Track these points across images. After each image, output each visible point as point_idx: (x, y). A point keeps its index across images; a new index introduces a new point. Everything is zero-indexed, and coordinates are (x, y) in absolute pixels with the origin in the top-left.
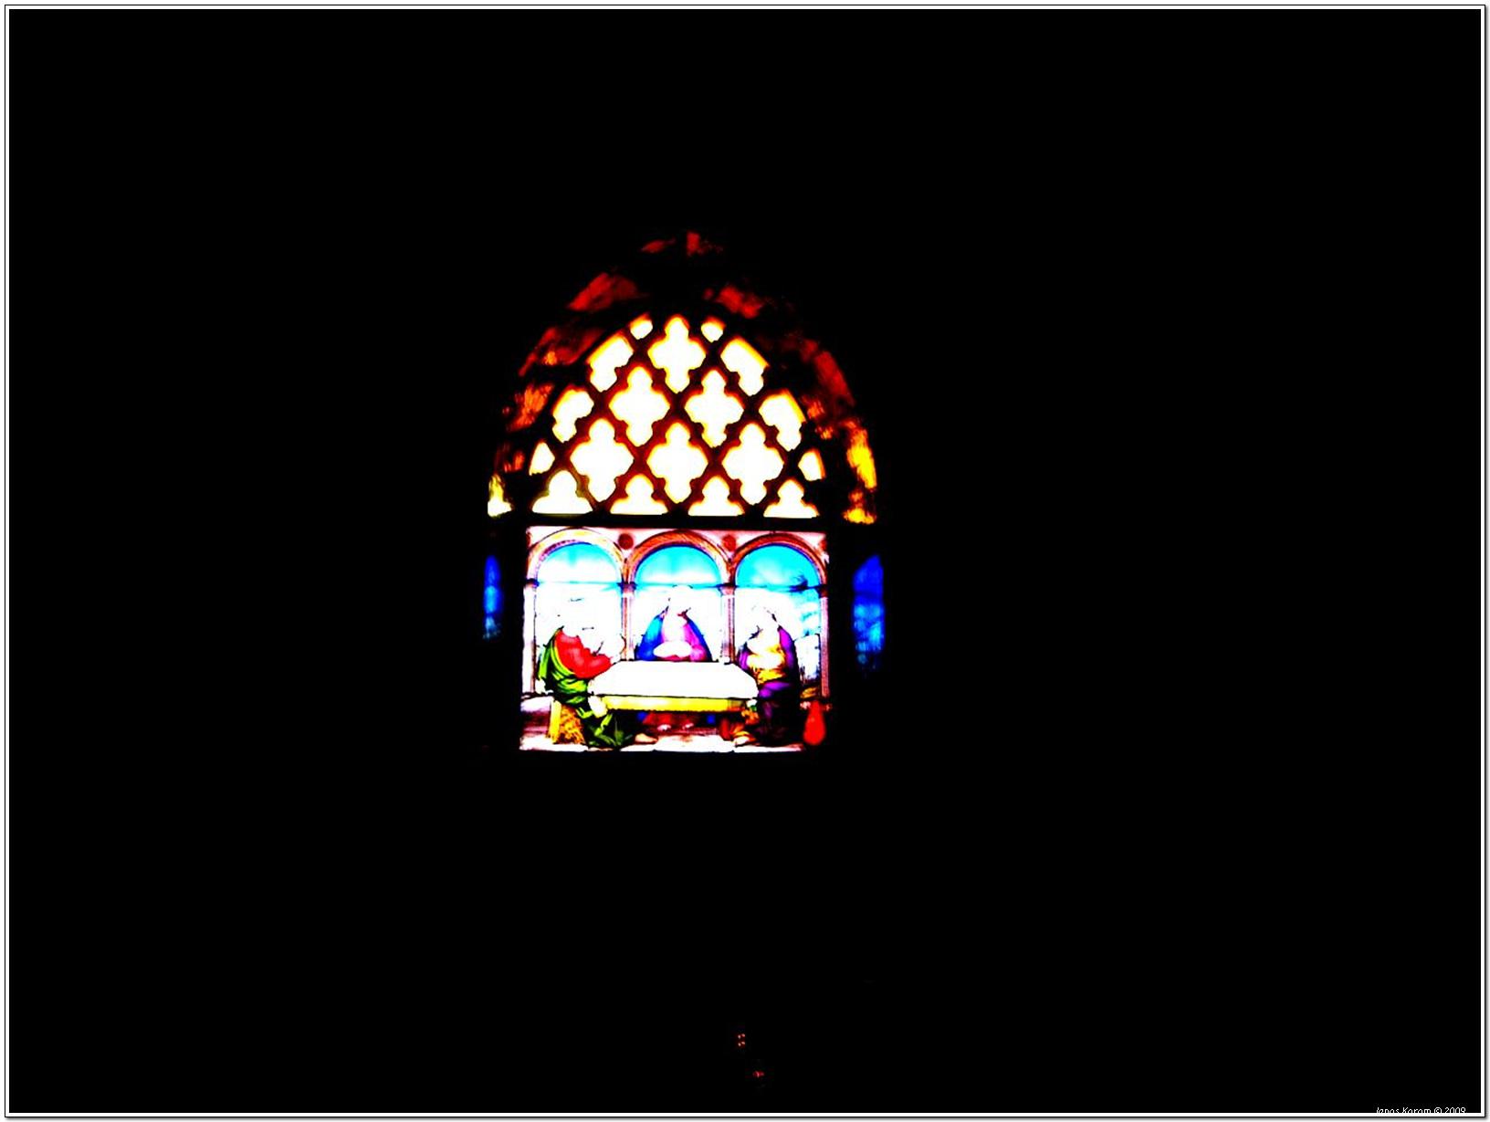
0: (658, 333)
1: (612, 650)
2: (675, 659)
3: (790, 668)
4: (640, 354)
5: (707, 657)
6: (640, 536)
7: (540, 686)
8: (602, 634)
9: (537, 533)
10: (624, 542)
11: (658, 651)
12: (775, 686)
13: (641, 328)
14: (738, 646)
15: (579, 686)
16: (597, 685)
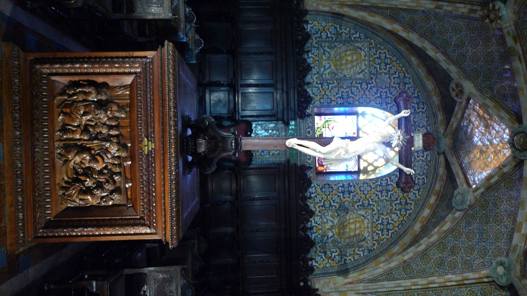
7: (327, 119)
15: (327, 126)
16: (327, 129)
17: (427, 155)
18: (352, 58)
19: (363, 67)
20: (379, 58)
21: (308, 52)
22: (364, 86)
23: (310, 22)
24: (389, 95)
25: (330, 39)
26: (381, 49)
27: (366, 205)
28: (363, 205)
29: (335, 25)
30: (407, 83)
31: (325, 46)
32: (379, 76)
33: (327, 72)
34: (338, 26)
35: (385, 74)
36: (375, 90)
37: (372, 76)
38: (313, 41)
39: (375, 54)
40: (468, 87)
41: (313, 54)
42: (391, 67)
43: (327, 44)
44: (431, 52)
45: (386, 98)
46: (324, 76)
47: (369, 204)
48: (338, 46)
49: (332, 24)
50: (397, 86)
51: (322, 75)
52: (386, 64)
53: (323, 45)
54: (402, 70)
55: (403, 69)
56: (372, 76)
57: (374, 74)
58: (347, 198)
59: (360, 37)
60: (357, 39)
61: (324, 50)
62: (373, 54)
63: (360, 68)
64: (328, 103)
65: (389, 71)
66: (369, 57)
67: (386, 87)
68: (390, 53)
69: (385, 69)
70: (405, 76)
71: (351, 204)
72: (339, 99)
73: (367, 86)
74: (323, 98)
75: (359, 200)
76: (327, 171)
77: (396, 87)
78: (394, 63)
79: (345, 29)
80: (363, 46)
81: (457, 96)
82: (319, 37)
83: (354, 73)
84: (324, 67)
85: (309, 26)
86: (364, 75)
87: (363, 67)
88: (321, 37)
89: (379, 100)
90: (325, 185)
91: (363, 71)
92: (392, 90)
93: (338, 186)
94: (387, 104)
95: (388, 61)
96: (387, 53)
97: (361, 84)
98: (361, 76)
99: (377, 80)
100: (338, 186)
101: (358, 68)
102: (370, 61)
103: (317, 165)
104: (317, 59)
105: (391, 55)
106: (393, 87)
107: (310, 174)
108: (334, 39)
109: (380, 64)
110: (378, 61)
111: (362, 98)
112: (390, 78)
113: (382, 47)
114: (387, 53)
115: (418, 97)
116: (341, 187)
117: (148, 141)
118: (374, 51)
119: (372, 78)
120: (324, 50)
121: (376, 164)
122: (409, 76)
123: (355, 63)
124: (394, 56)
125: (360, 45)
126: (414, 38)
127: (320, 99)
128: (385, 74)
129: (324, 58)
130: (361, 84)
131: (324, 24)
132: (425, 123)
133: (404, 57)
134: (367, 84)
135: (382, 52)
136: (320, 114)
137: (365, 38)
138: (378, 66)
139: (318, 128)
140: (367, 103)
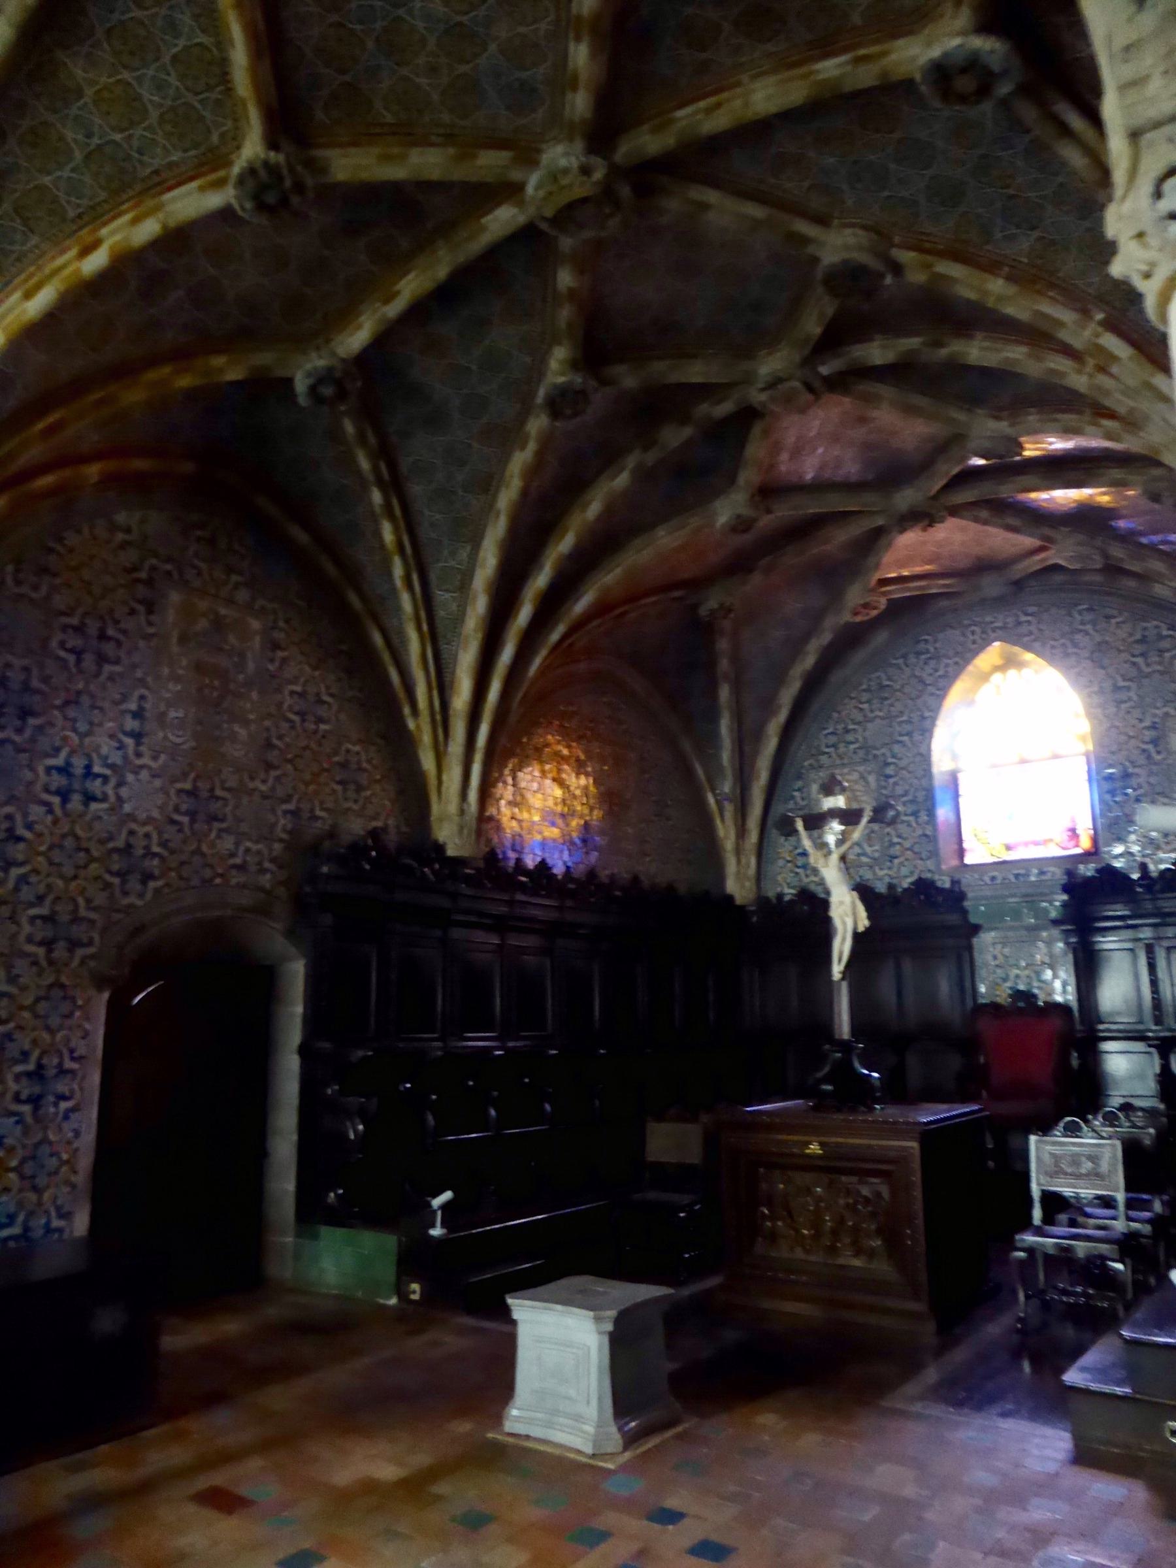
17: (1027, 614)
19: (855, 776)
22: (890, 770)
27: (1153, 733)
28: (1155, 742)
33: (868, 850)
40: (854, 595)
44: (809, 661)
46: (876, 855)
47: (1154, 727)
51: (875, 859)
57: (867, 753)
58: (1141, 780)
59: (799, 790)
71: (1154, 768)
72: (920, 820)
75: (1144, 751)
81: (875, 608)
84: (859, 855)
86: (869, 773)
87: (855, 776)
89: (917, 737)
91: (862, 777)
94: (923, 718)
97: (888, 777)
98: (872, 779)
103: (1078, 851)
107: (1087, 870)
110: (842, 749)
112: (871, 720)
115: (904, 656)
118: (824, 759)
119: (875, 756)
124: (830, 717)
126: (787, 697)
130: (888, 777)
131: (781, 863)
132: (957, 632)
134: (887, 764)
136: (961, 852)
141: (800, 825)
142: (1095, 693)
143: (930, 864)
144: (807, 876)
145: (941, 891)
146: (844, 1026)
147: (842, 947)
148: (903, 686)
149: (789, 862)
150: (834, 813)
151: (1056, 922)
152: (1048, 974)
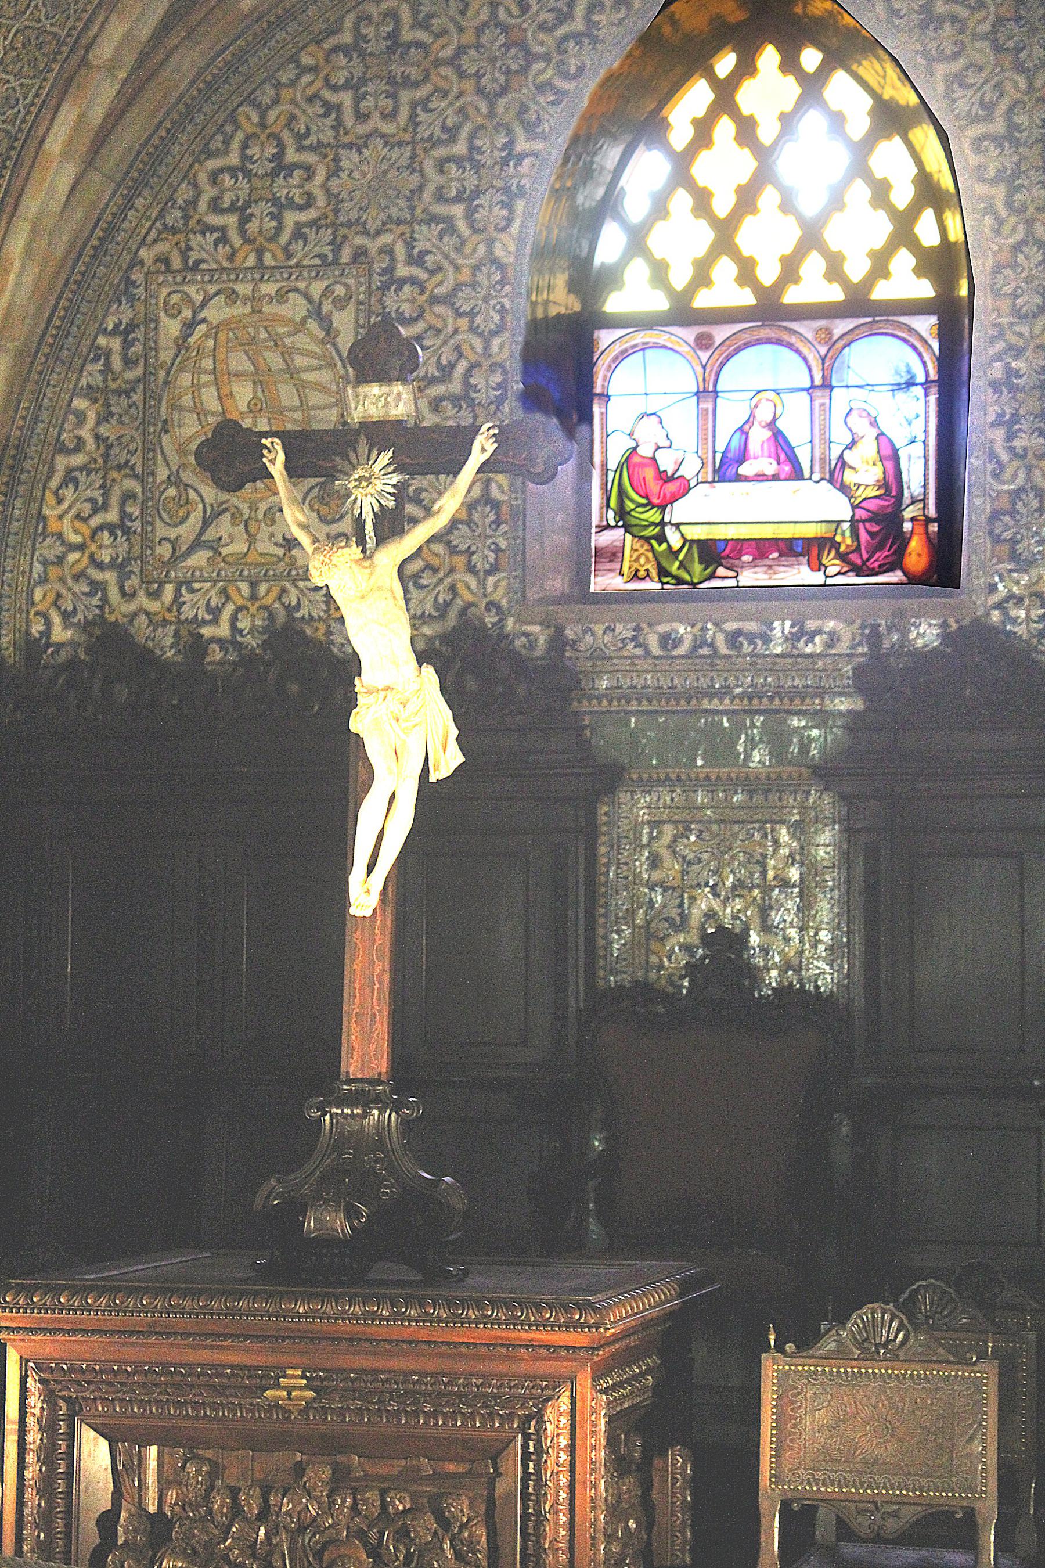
0: (746, 68)
1: (689, 470)
2: (760, 478)
3: (892, 485)
4: (725, 95)
5: (797, 474)
6: (721, 333)
8: (681, 451)
9: (605, 338)
10: (703, 342)
11: (745, 469)
12: (872, 505)
13: (725, 64)
14: (835, 454)
15: (654, 516)
16: (679, 511)
18: (238, 375)
19: (296, 308)
20: (242, 210)
21: (198, 646)
23: (37, 628)
24: (460, 148)
25: (134, 510)
26: (194, 202)
29: (54, 484)
30: (393, 36)
31: (174, 543)
32: (349, 211)
34: (62, 462)
35: (335, 172)
36: (426, 236)
37: (346, 257)
38: (139, 610)
39: (224, 240)
41: (215, 612)
42: (299, 137)
43: (161, 530)
45: (478, 167)
48: (174, 459)
49: (50, 498)
50: (405, 96)
52: (280, 167)
53: (165, 551)
54: (315, 69)
55: (306, 60)
56: (346, 257)
60: (138, 348)
61: (196, 545)
62: (223, 250)
63: (300, 327)
64: (497, 523)
65: (318, 148)
66: (238, 273)
67: (413, 166)
68: (217, 144)
69: (309, 171)
70: (346, 50)
73: (402, 282)
74: (469, 553)
76: (932, 512)
77: (414, 105)
78: (272, 116)
79: (81, 418)
80: (173, 312)
82: (123, 577)
83: (331, 365)
85: (60, 634)
86: (340, 303)
87: (296, 308)
88: (120, 567)
90: (997, 540)
92: (429, 125)
93: (1005, 457)
95: (262, 152)
96: (212, 164)
99: (373, 219)
100: (1005, 457)
101: (301, 340)
102: (260, 264)
104: (245, 588)
105: (227, 142)
106: (413, 120)
108: (131, 484)
109: (280, 207)
110: (261, 222)
111: (471, 314)
113: (184, 193)
114: (212, 164)
116: (1010, 437)
117: (278, 1386)
118: (201, 245)
119: (360, 254)
120: (196, 545)
121: (903, 195)
122: (349, 21)
123: (274, 360)
124: (232, 118)
125: (171, 328)
127: (471, 569)
128: (335, 172)
129: (240, 547)
131: (49, 549)
133: (241, 57)
134: (392, 282)
135: (209, 192)
137: (132, 300)
138: (291, 218)
139: (663, 572)
140: (502, 282)
141: (277, 463)
142: (997, 140)
143: (498, 588)
144: (128, 595)
145: (519, 664)
146: (366, 1047)
147: (384, 822)
148: (460, 51)
149: (73, 547)
150: (380, 434)
151: (824, 773)
152: (786, 913)
